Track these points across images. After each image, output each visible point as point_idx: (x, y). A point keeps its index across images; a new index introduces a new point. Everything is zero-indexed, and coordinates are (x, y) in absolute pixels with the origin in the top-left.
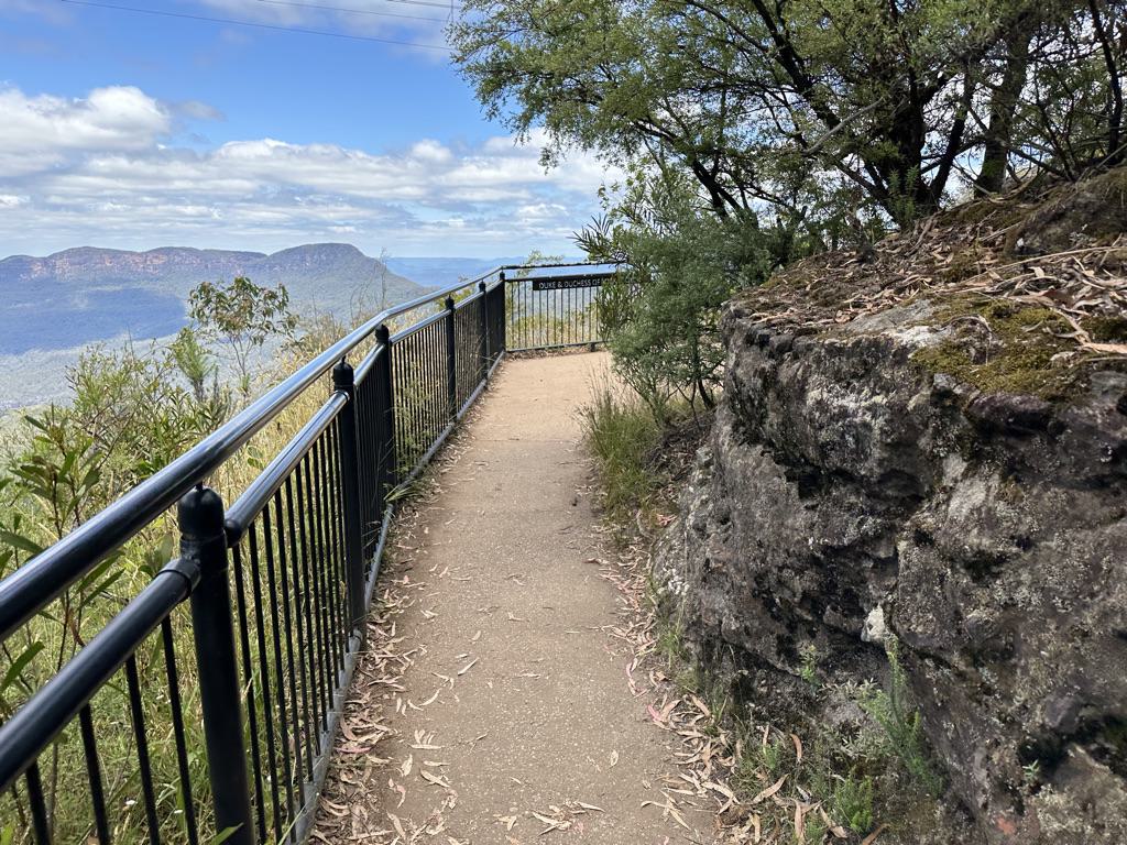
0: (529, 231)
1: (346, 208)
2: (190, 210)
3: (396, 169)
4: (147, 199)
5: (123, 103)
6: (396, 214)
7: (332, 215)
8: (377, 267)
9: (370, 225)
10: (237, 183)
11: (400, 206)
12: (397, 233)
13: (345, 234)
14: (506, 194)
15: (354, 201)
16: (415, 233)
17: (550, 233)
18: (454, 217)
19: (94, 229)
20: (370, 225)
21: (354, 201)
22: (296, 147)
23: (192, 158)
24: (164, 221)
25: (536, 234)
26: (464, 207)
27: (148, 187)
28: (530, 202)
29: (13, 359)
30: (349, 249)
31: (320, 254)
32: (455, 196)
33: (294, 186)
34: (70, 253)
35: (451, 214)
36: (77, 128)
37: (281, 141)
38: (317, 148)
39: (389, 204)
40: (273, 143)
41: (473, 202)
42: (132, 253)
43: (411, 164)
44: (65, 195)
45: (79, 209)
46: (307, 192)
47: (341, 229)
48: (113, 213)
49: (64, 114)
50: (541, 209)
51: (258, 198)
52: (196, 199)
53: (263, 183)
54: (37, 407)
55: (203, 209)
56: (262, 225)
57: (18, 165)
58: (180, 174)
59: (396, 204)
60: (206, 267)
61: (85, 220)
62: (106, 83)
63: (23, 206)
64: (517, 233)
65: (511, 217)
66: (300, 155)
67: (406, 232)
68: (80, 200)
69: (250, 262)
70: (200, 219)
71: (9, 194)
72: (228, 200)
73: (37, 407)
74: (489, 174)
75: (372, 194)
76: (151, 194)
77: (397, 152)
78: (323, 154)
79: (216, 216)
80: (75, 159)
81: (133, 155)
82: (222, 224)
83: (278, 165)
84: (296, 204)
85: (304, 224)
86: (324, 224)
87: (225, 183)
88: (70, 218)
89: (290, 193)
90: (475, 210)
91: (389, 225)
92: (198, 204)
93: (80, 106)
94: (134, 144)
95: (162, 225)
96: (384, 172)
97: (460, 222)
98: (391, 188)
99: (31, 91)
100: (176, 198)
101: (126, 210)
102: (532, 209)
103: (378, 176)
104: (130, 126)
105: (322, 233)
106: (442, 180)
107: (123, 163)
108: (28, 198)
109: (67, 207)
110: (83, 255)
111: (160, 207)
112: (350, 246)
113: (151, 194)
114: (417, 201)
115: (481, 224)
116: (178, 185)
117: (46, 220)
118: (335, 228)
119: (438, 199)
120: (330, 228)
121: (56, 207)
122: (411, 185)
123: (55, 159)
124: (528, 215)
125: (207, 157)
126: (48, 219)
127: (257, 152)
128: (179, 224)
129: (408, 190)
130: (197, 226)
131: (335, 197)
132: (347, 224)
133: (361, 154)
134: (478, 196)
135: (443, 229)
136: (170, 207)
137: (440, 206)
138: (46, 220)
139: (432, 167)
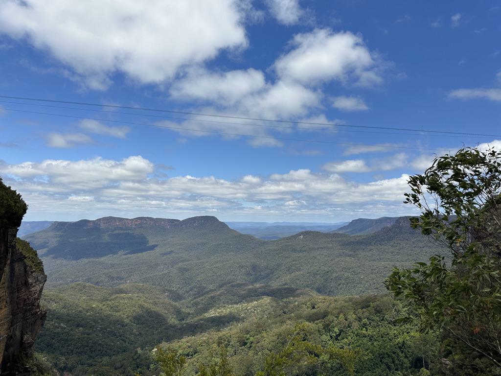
0: (289, 211)
1: (216, 202)
2: (154, 202)
3: (237, 187)
4: (138, 198)
5: (136, 162)
6: (233, 204)
7: (210, 204)
8: (223, 225)
9: (223, 209)
10: (173, 192)
11: (238, 201)
12: (234, 212)
13: (212, 212)
14: (280, 196)
15: (218, 199)
16: (240, 211)
17: (298, 212)
18: (258, 206)
19: (115, 210)
20: (223, 209)
21: (218, 199)
22: (199, 179)
23: (157, 183)
24: (143, 207)
25: (291, 212)
26: (262, 201)
27: (140, 194)
28: (292, 200)
29: (75, 262)
30: (213, 219)
31: (201, 220)
32: (257, 198)
33: (195, 193)
34: (104, 219)
35: (257, 204)
36: (119, 171)
37: (192, 176)
38: (206, 179)
39: (232, 201)
40: (189, 177)
41: (266, 200)
42: (127, 219)
43: (243, 185)
44: (108, 197)
45: (110, 202)
46: (201, 196)
47: (211, 210)
48: (122, 204)
49: (112, 166)
50: (294, 202)
51: (182, 198)
52: (154, 198)
53: (184, 192)
54: (80, 282)
55: (158, 202)
56: (181, 208)
57: (93, 185)
58: (154, 188)
59: (236, 201)
60: (156, 225)
61: (113, 206)
62: (127, 157)
63: (91, 201)
64: (285, 212)
65: (283, 205)
66: (199, 181)
67: (237, 211)
68: (112, 198)
69: (173, 224)
70: (158, 206)
71: (88, 196)
72: (169, 199)
73: (80, 282)
74: (274, 188)
75: (224, 197)
76: (142, 196)
77: (236, 180)
78: (207, 181)
79: (164, 205)
80: (114, 183)
81: (134, 181)
82: (165, 208)
83: (191, 185)
84: (196, 200)
85: (196, 208)
86: (205, 208)
87: (168, 192)
88: (108, 205)
89: (194, 197)
90: (266, 202)
91: (230, 209)
92: (157, 200)
93: (121, 164)
94: (139, 177)
95: (142, 208)
96: (233, 188)
97: (259, 208)
98: (235, 194)
99: (106, 157)
100: (147, 198)
101: (129, 203)
102: (291, 203)
103: (230, 190)
104: (137, 171)
105: (204, 212)
106: (253, 191)
107: (131, 184)
108: (93, 197)
109: (107, 201)
110: (111, 219)
111: (143, 201)
112: (214, 217)
113: (142, 196)
114: (243, 199)
115: (268, 208)
116: (152, 193)
117: (99, 206)
118: (209, 210)
119: (251, 198)
120: (207, 210)
121: (103, 201)
122: (240, 193)
123: (106, 182)
124: (289, 205)
125: (163, 183)
126: (99, 206)
127: (184, 182)
128: (149, 208)
129: (239, 195)
130: (156, 209)
131: (209, 197)
132: (214, 208)
133: (222, 181)
134: (268, 197)
135: (253, 210)
136: (145, 201)
137: (253, 201)
138: (99, 206)
139: (253, 186)
